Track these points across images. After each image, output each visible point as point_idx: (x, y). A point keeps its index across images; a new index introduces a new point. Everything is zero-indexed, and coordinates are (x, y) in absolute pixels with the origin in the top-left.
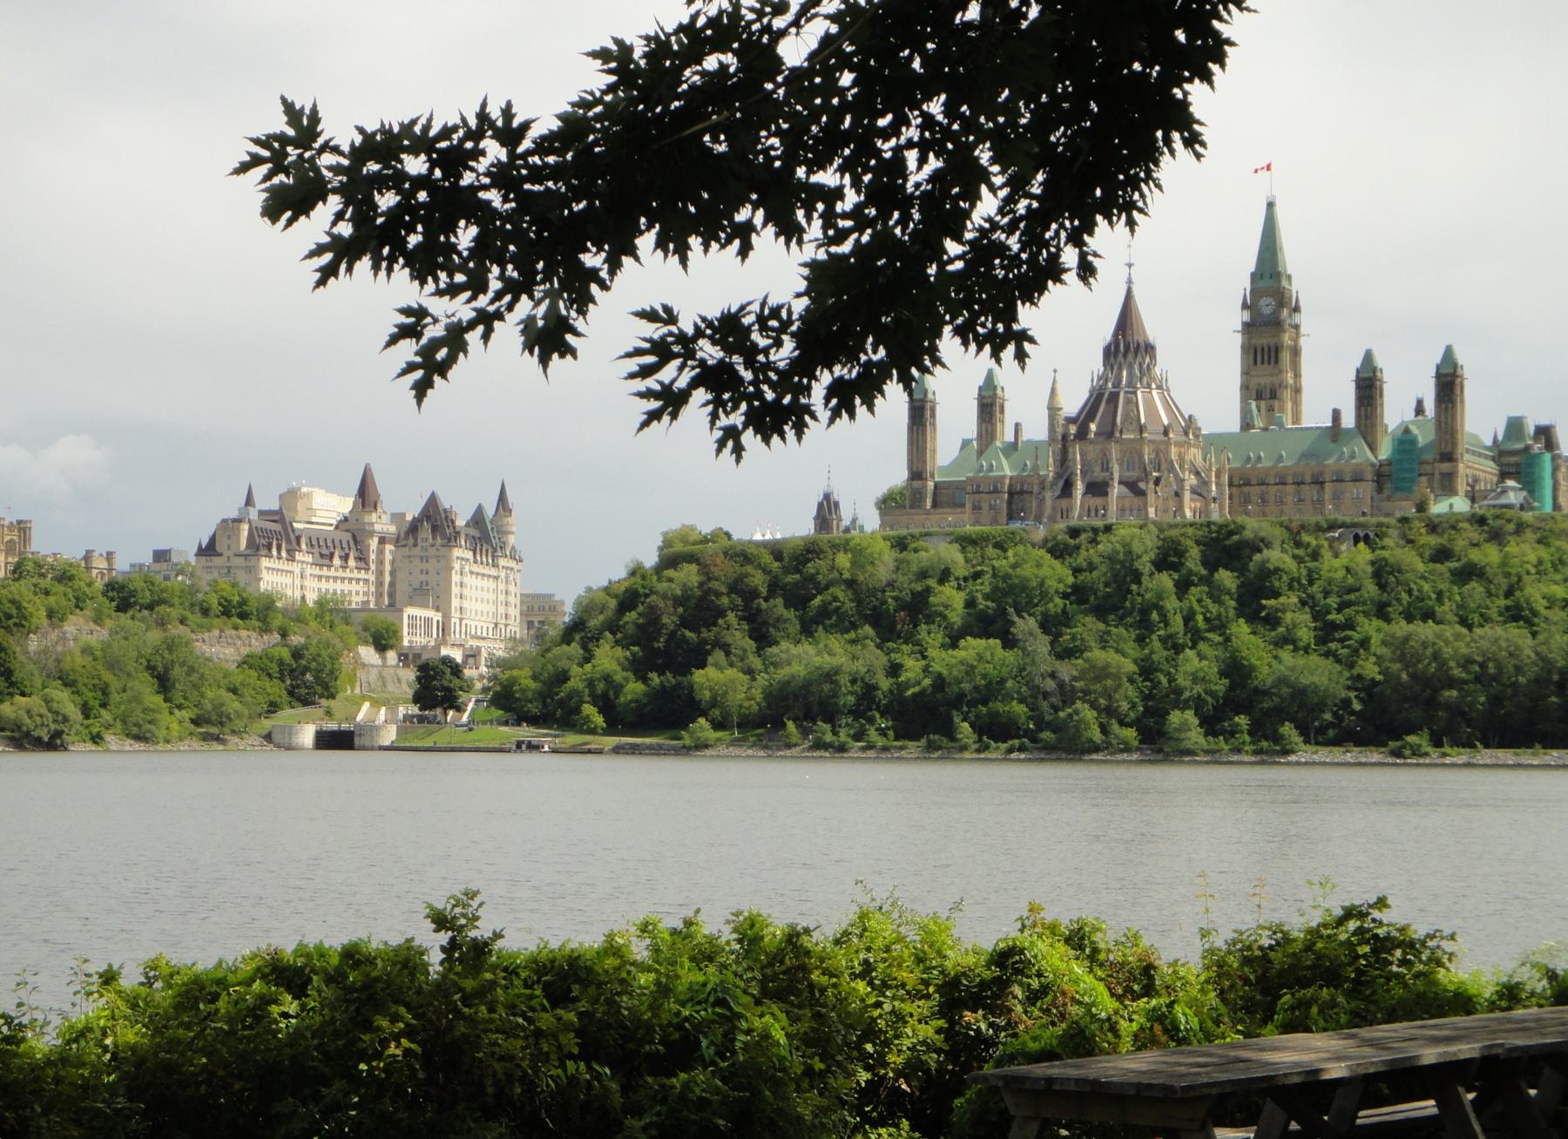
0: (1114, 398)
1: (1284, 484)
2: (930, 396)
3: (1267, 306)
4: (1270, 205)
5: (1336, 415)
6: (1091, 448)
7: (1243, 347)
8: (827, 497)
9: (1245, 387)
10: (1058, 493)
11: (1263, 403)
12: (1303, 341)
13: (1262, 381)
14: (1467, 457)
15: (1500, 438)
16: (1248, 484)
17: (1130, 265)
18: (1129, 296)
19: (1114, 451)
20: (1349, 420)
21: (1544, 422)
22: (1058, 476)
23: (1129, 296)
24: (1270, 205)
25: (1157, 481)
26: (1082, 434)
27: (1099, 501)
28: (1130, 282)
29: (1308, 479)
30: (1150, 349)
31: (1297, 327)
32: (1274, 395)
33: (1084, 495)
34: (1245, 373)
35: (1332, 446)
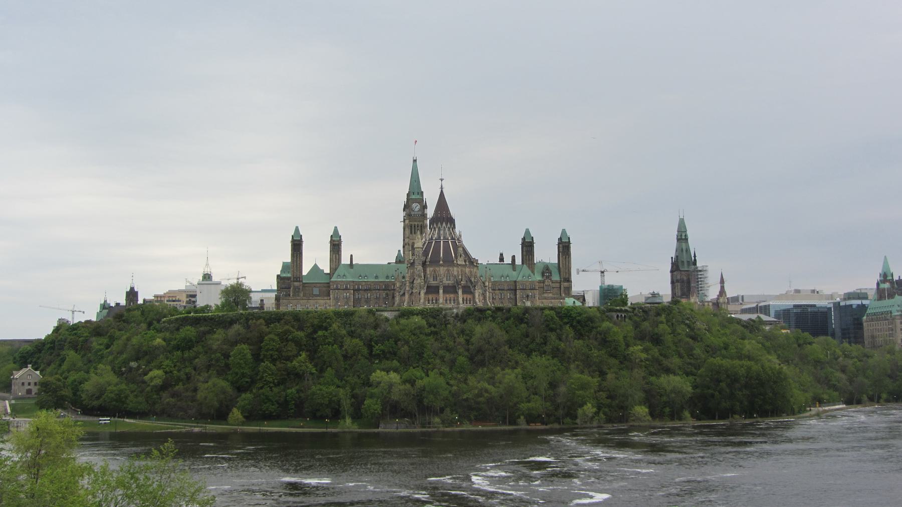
4: (415, 161)
5: (514, 257)
6: (442, 268)
8: (132, 289)
17: (442, 180)
18: (442, 195)
19: (455, 271)
20: (519, 261)
23: (442, 195)
24: (415, 161)
27: (452, 296)
35: (514, 273)
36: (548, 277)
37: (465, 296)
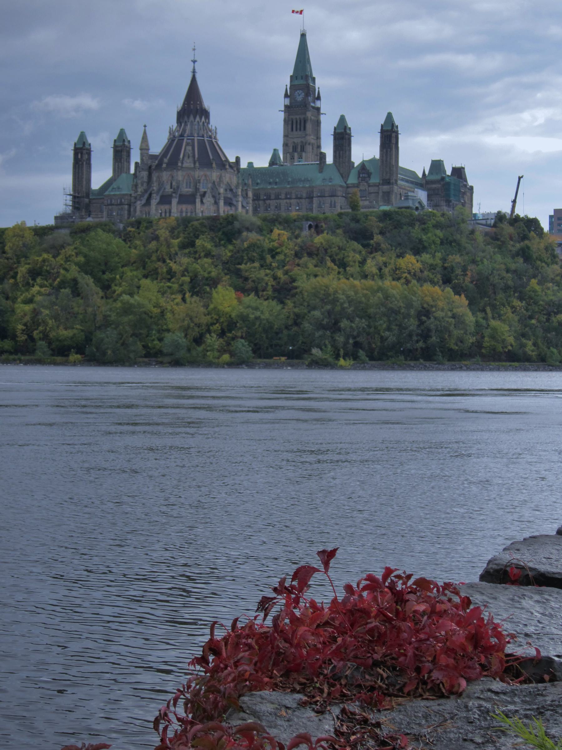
0: (180, 142)
1: (290, 198)
2: (87, 146)
3: (300, 97)
4: (303, 36)
7: (285, 121)
9: (285, 145)
10: (144, 201)
11: (296, 155)
12: (322, 118)
13: (296, 140)
14: (399, 182)
15: (427, 173)
16: (269, 198)
17: (194, 62)
18: (194, 81)
21: (458, 165)
22: (146, 191)
23: (194, 81)
24: (303, 36)
25: (204, 195)
26: (159, 166)
27: (167, 207)
28: (194, 72)
29: (304, 195)
30: (205, 114)
31: (318, 109)
32: (303, 149)
33: (159, 203)
34: (286, 136)
35: (319, 175)
36: (363, 179)
37: (180, 207)
